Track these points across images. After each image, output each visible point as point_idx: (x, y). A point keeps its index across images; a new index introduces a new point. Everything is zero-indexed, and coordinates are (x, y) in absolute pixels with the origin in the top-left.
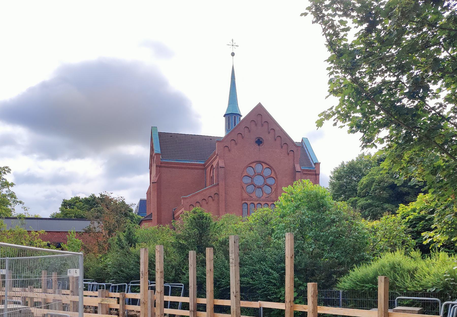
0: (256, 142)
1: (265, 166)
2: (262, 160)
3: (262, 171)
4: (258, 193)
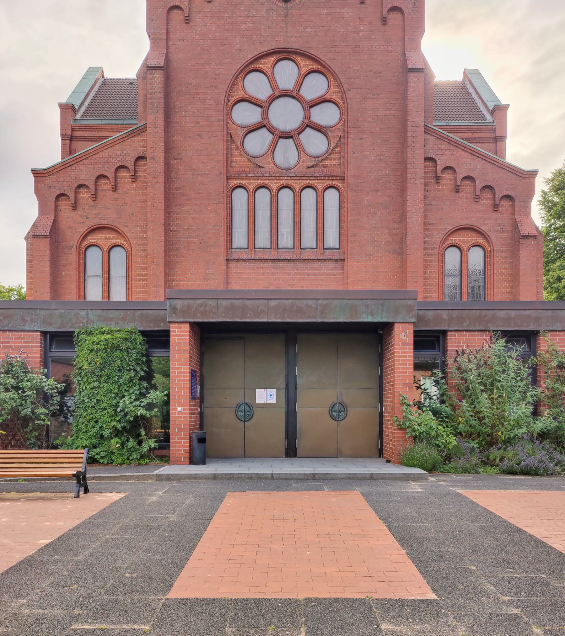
1: (307, 65)
2: (294, 44)
3: (299, 84)
4: (286, 155)
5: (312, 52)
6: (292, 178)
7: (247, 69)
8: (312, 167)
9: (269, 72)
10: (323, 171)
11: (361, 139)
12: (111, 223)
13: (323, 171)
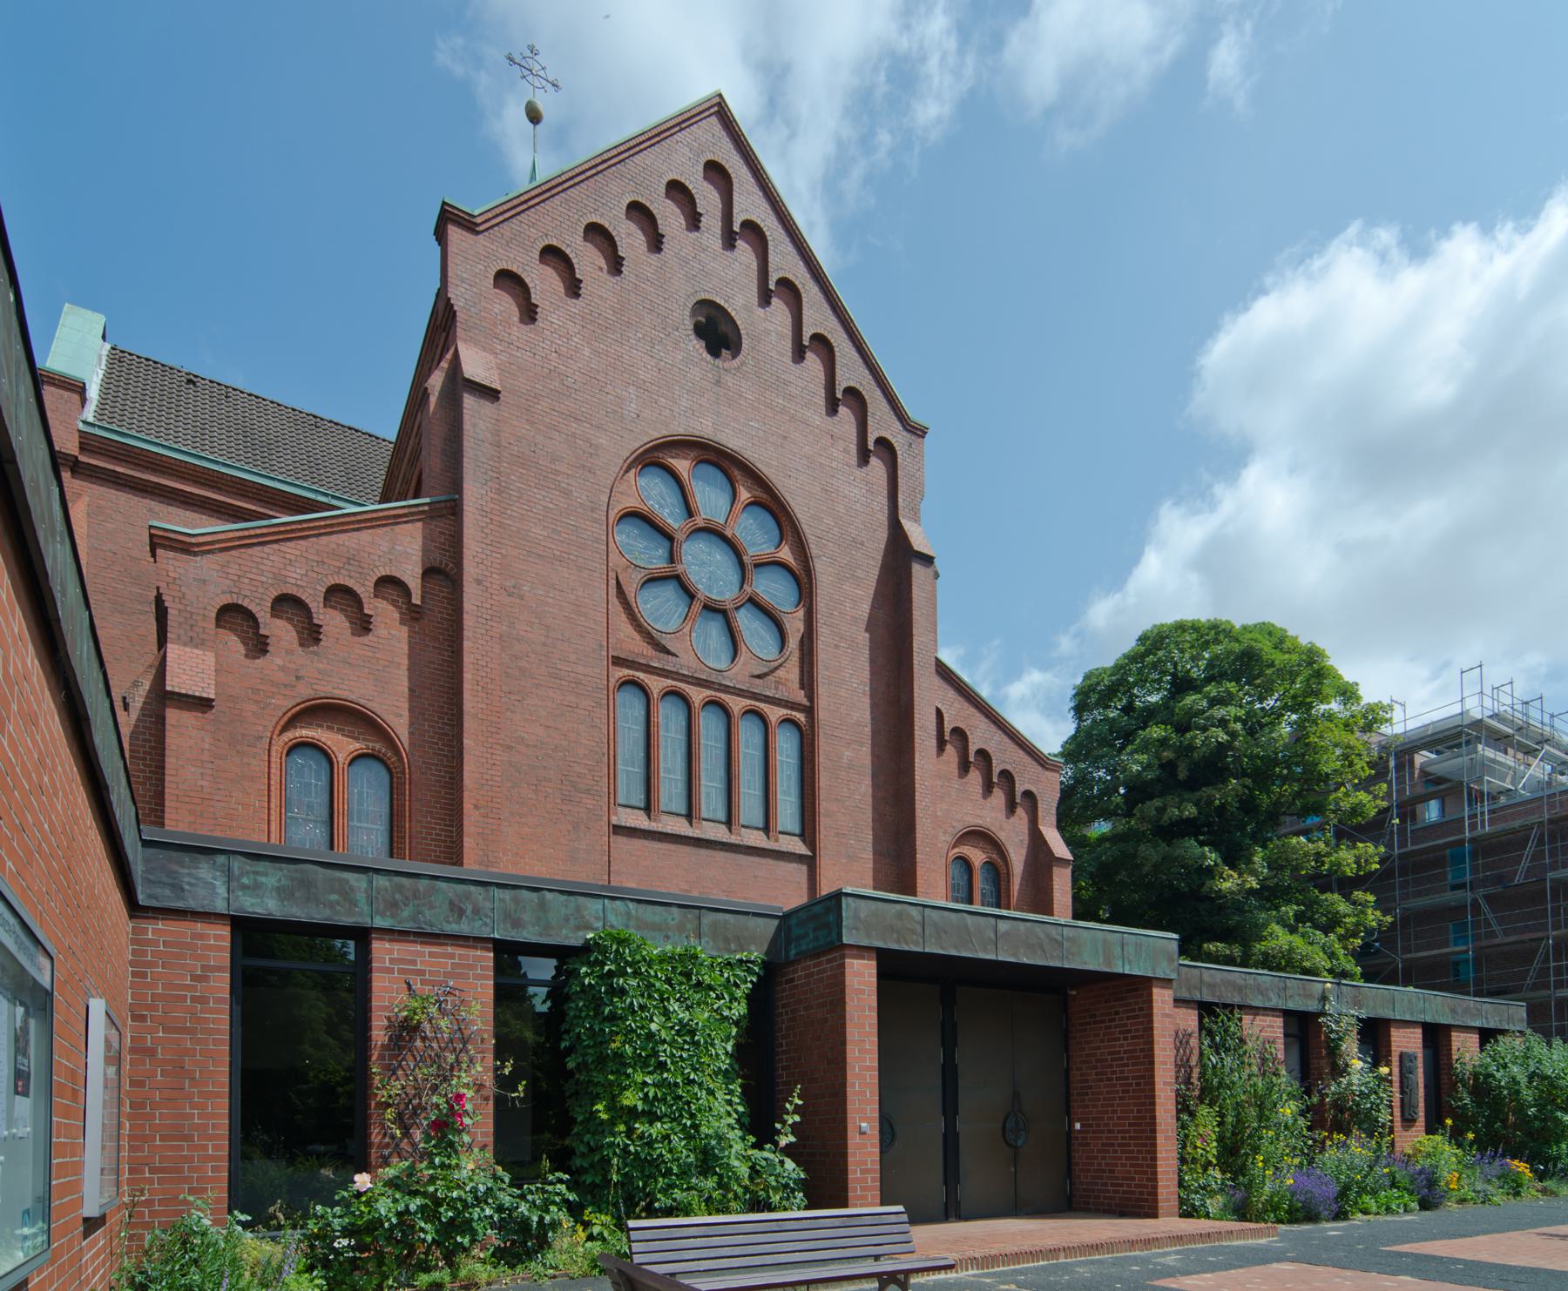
8: (759, 677)
12: (362, 701)
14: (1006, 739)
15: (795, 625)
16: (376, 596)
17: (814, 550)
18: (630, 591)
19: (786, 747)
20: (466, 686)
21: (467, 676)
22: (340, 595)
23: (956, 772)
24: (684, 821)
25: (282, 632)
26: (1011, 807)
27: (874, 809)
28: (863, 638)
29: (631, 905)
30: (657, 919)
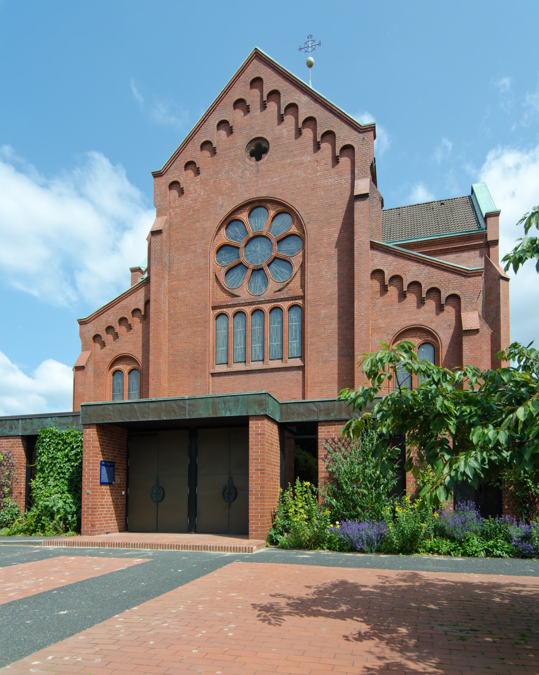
0: (265, 151)
2: (263, 194)
5: (277, 197)
6: (262, 302)
7: (228, 221)
8: (279, 291)
9: (245, 219)
10: (287, 293)
11: (318, 261)
13: (287, 293)
14: (433, 270)
15: (296, 261)
16: (133, 317)
17: (305, 220)
18: (222, 278)
19: (292, 320)
20: (151, 338)
21: (151, 335)
22: (123, 320)
23: (397, 299)
24: (243, 364)
25: (108, 338)
26: (440, 308)
27: (339, 334)
28: (334, 252)
29: (57, 418)
30: (65, 421)
